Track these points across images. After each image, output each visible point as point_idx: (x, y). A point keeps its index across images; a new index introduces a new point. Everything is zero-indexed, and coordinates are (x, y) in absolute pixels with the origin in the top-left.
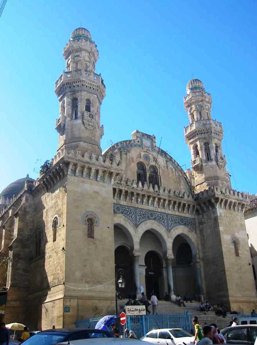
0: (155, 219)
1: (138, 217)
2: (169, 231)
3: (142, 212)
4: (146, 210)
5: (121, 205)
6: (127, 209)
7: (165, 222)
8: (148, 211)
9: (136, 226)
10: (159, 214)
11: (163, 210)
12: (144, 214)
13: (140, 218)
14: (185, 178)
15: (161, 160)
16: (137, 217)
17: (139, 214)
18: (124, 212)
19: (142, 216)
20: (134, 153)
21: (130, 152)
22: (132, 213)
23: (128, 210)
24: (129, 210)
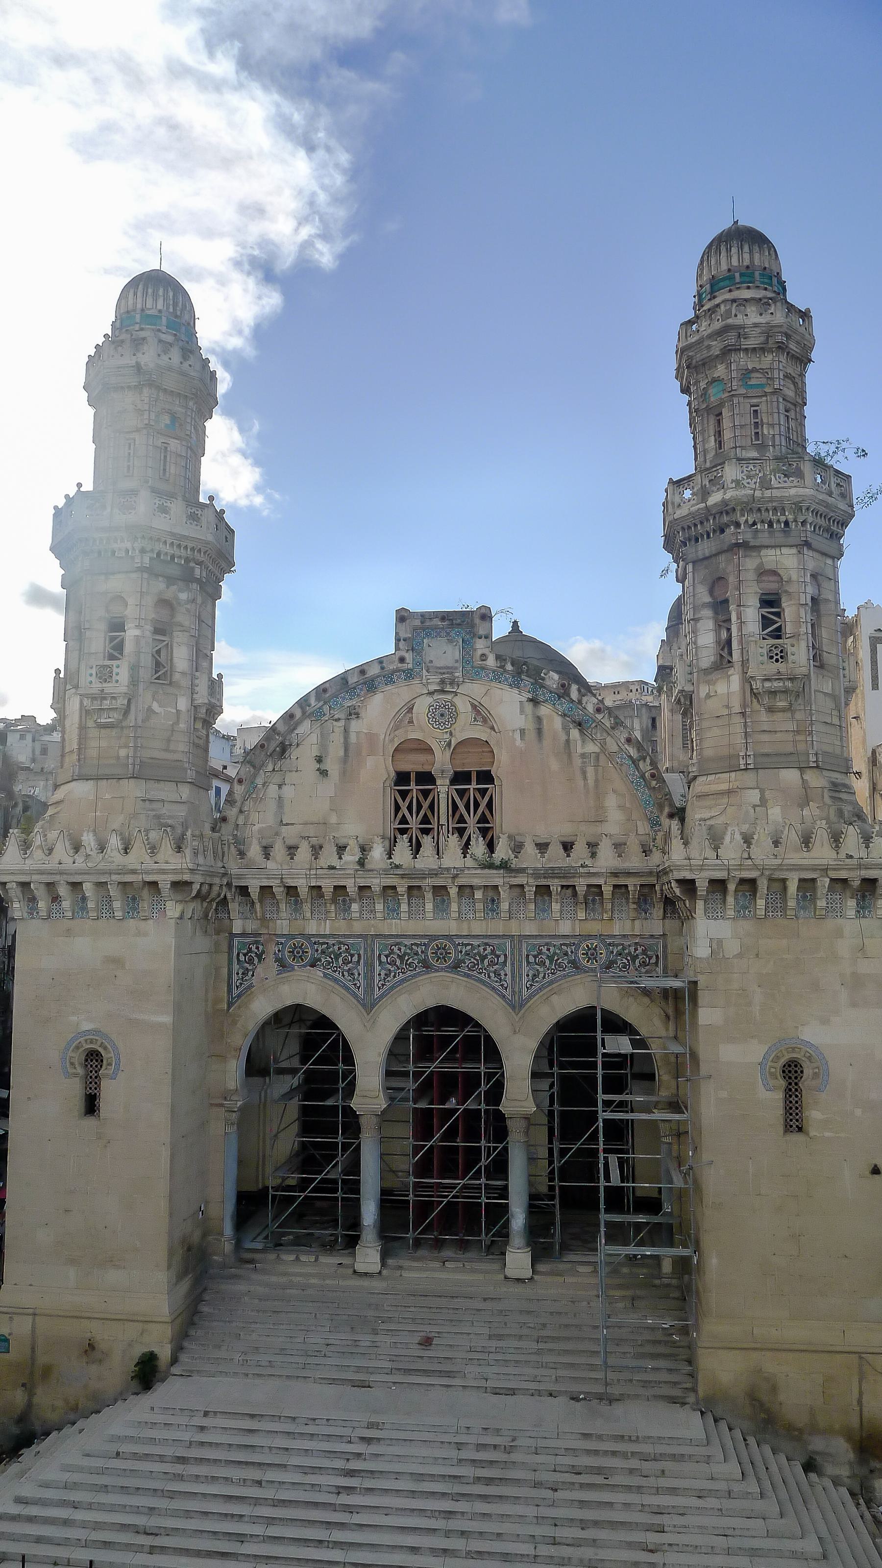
0: (456, 967)
1: (378, 968)
2: (517, 1005)
3: (400, 949)
4: (414, 936)
5: (308, 937)
6: (334, 945)
7: (502, 973)
8: (426, 941)
9: (369, 1005)
10: (476, 942)
11: (497, 927)
12: (405, 954)
13: (386, 975)
14: (630, 757)
15: (509, 705)
16: (373, 970)
17: (384, 959)
18: (320, 960)
19: (398, 962)
20: (377, 711)
21: (362, 715)
22: (355, 959)
23: (339, 948)
24: (343, 948)
